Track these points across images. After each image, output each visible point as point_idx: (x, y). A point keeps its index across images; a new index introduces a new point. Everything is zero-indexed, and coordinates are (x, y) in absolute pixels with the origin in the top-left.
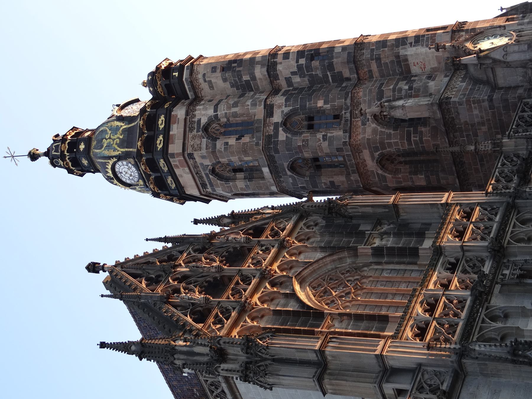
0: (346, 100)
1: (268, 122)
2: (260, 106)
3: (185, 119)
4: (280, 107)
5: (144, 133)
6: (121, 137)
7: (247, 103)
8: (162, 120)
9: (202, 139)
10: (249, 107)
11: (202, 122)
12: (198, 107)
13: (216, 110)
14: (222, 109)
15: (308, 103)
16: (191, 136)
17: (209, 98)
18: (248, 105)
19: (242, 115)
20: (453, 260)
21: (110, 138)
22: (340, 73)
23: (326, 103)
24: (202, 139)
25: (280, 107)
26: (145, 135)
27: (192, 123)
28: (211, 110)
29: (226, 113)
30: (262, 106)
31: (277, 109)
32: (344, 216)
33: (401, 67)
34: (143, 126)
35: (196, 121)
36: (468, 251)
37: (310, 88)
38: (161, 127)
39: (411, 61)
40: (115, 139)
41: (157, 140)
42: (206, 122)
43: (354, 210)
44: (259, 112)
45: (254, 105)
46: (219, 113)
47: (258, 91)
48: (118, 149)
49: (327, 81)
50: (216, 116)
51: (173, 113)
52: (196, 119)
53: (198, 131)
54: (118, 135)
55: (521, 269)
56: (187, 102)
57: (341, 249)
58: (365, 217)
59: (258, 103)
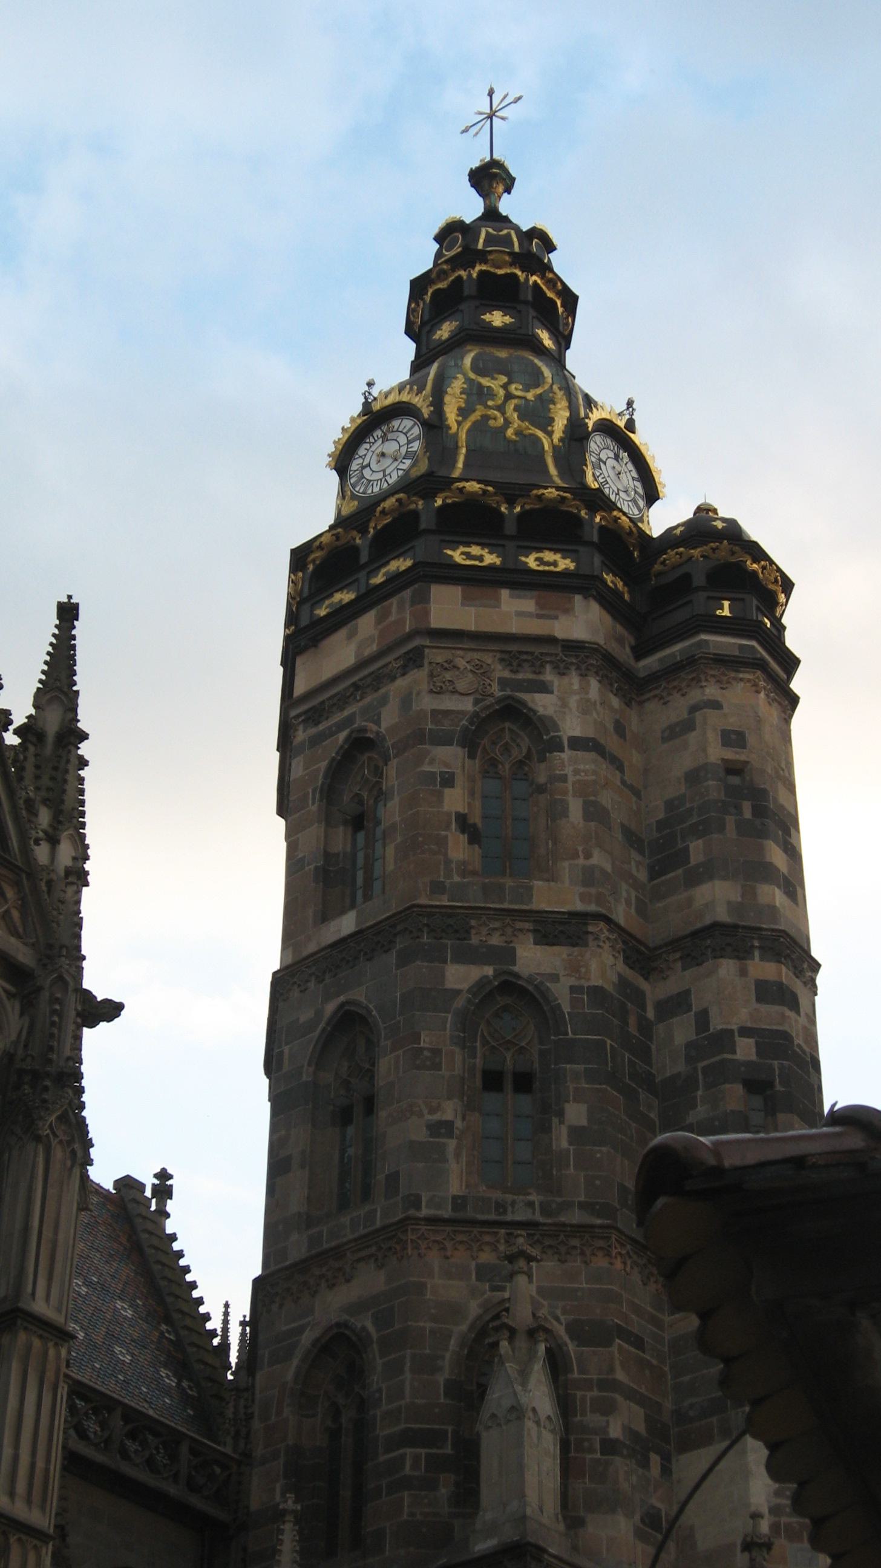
0: (582, 1206)
1: (519, 925)
2: (583, 897)
4: (574, 968)
5: (511, 503)
6: (510, 432)
7: (596, 853)
8: (555, 564)
9: (471, 699)
10: (581, 861)
11: (538, 696)
12: (594, 684)
13: (577, 743)
14: (582, 767)
15: (581, 1067)
16: (488, 659)
17: (634, 723)
18: (588, 856)
21: (509, 396)
23: (577, 1134)
24: (471, 699)
25: (574, 968)
26: (503, 509)
28: (579, 728)
29: (564, 779)
30: (579, 906)
31: (565, 956)
34: (540, 498)
35: (541, 677)
38: (531, 561)
40: (503, 413)
41: (483, 545)
42: (535, 712)
45: (589, 877)
46: (566, 755)
48: (467, 425)
50: (556, 745)
51: (578, 598)
52: (549, 675)
53: (503, 683)
54: (516, 423)
56: (624, 654)
59: (593, 891)
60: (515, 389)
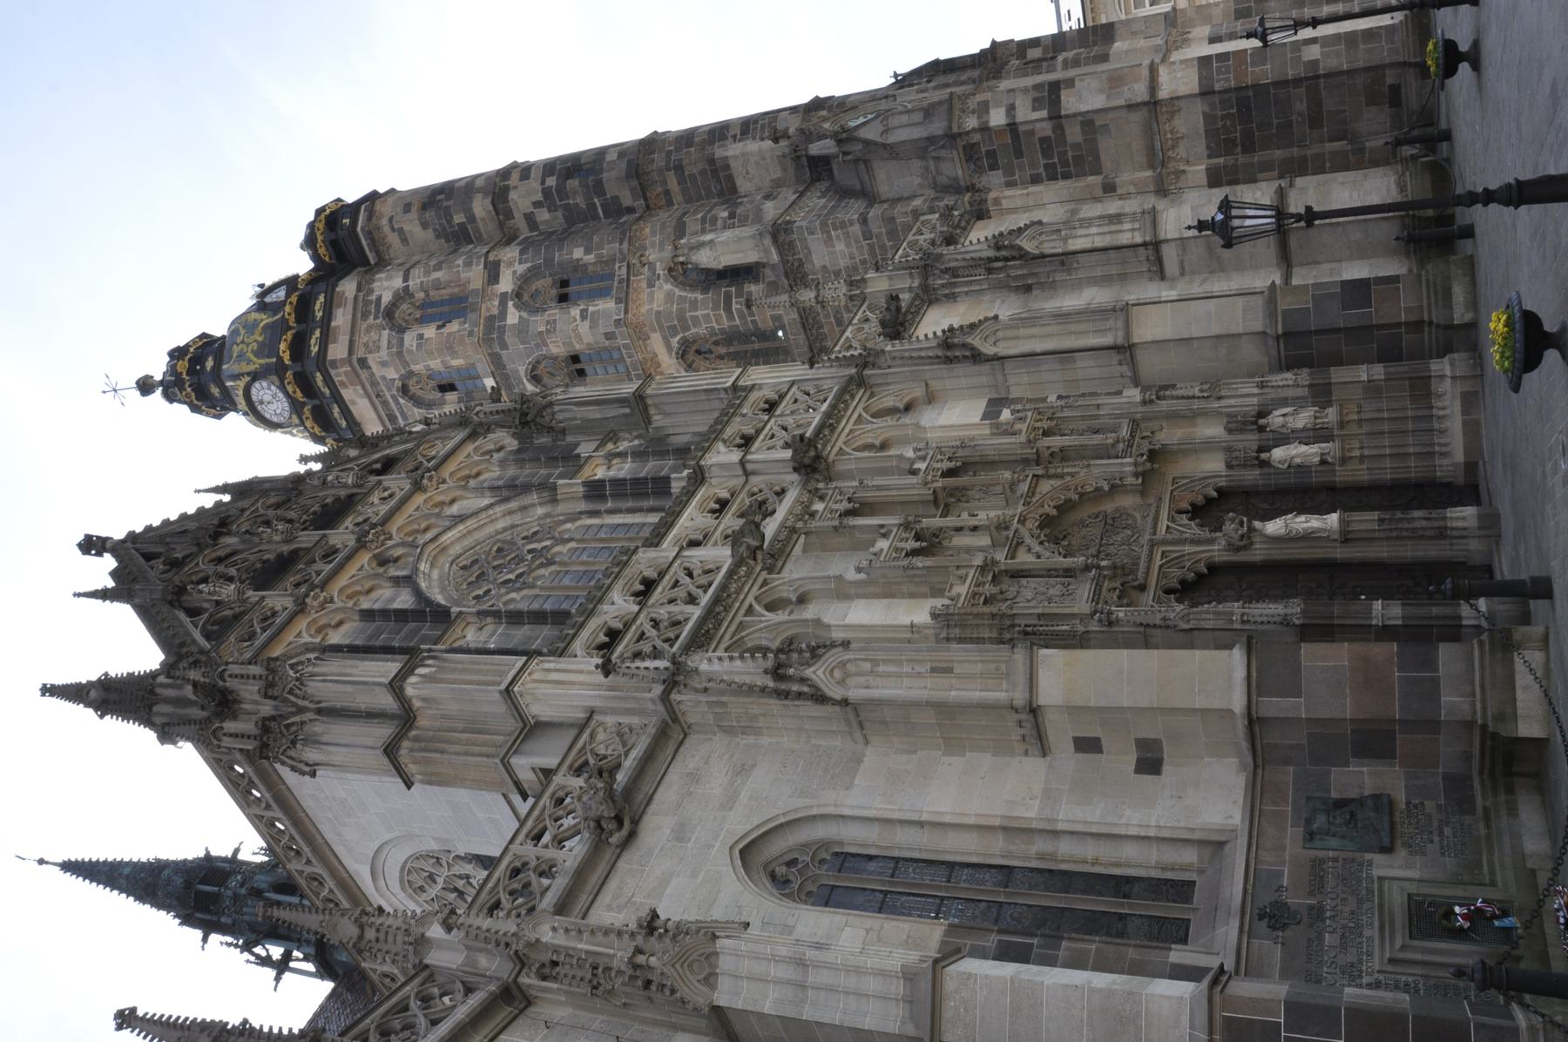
2: (477, 265)
3: (356, 298)
6: (260, 339)
13: (406, 279)
19: (448, 284)
20: (724, 494)
22: (616, 199)
26: (293, 331)
27: (367, 303)
29: (422, 282)
30: (482, 266)
32: (551, 429)
33: (719, 180)
36: (754, 473)
37: (565, 230)
39: (736, 168)
43: (567, 415)
44: (474, 276)
46: (411, 283)
47: (480, 240)
49: (596, 217)
50: (406, 289)
52: (373, 297)
55: (850, 500)
57: (526, 488)
58: (587, 428)
60: (239, 340)
